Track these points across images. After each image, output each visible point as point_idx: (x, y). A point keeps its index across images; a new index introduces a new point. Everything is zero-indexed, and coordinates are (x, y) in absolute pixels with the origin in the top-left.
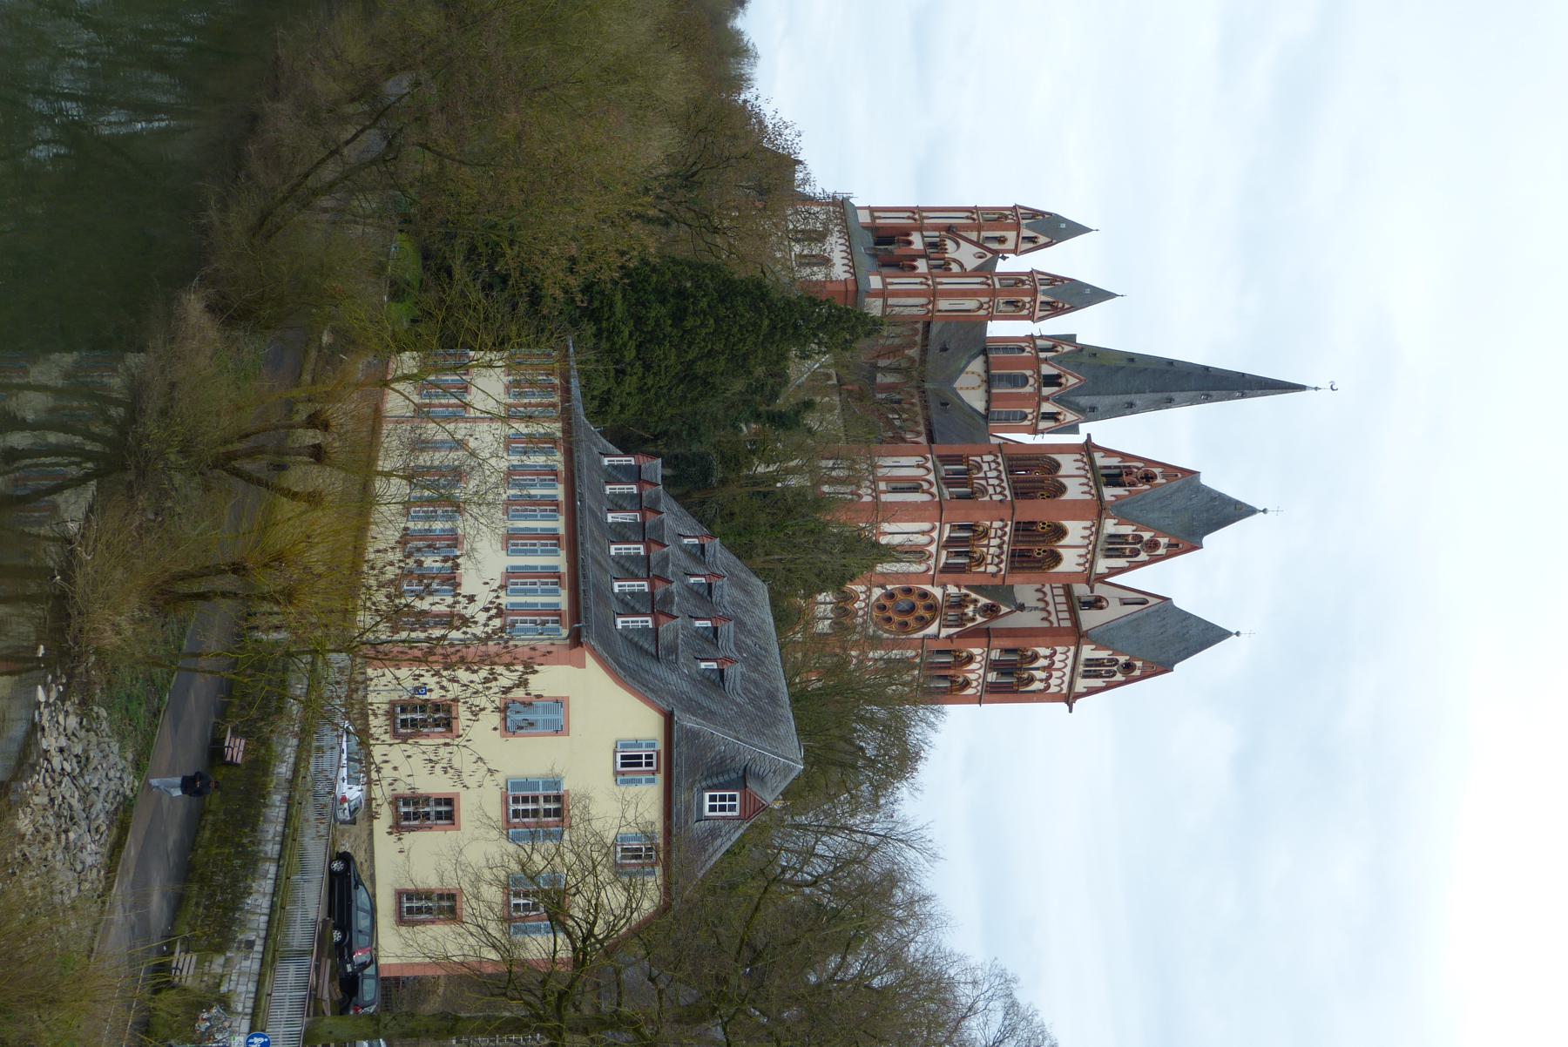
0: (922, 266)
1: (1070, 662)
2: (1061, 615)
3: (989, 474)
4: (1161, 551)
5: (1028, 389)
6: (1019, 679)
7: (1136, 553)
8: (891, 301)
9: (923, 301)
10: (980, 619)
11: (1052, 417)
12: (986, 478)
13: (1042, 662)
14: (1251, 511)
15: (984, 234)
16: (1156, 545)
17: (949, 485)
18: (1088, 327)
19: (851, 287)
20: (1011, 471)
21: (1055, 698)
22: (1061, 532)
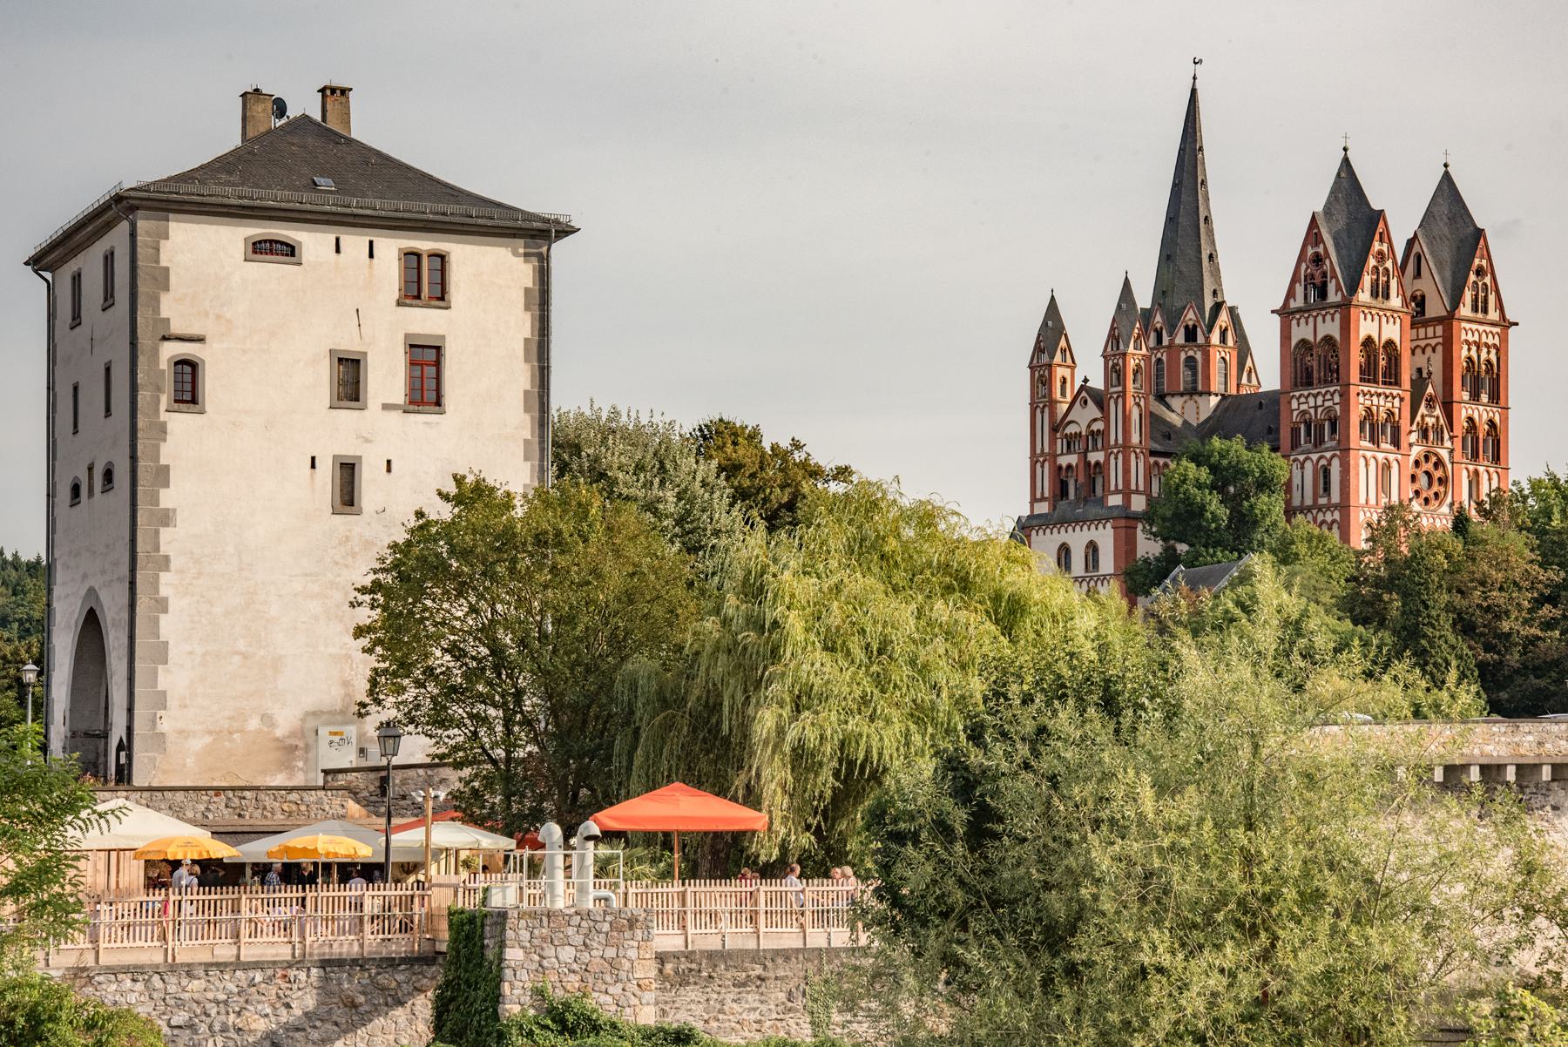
0: (1096, 457)
1: (1474, 326)
2: (1430, 334)
3: (1312, 403)
4: (1385, 248)
5: (1199, 356)
6: (1487, 372)
7: (1387, 270)
8: (1133, 487)
9: (1133, 456)
10: (1438, 412)
11: (1223, 333)
12: (1316, 407)
13: (1474, 353)
14: (1346, 161)
15: (1058, 395)
16: (1380, 253)
17: (1322, 441)
18: (1144, 299)
19: (1122, 523)
20: (1309, 383)
21: (1504, 339)
22: (1368, 341)
